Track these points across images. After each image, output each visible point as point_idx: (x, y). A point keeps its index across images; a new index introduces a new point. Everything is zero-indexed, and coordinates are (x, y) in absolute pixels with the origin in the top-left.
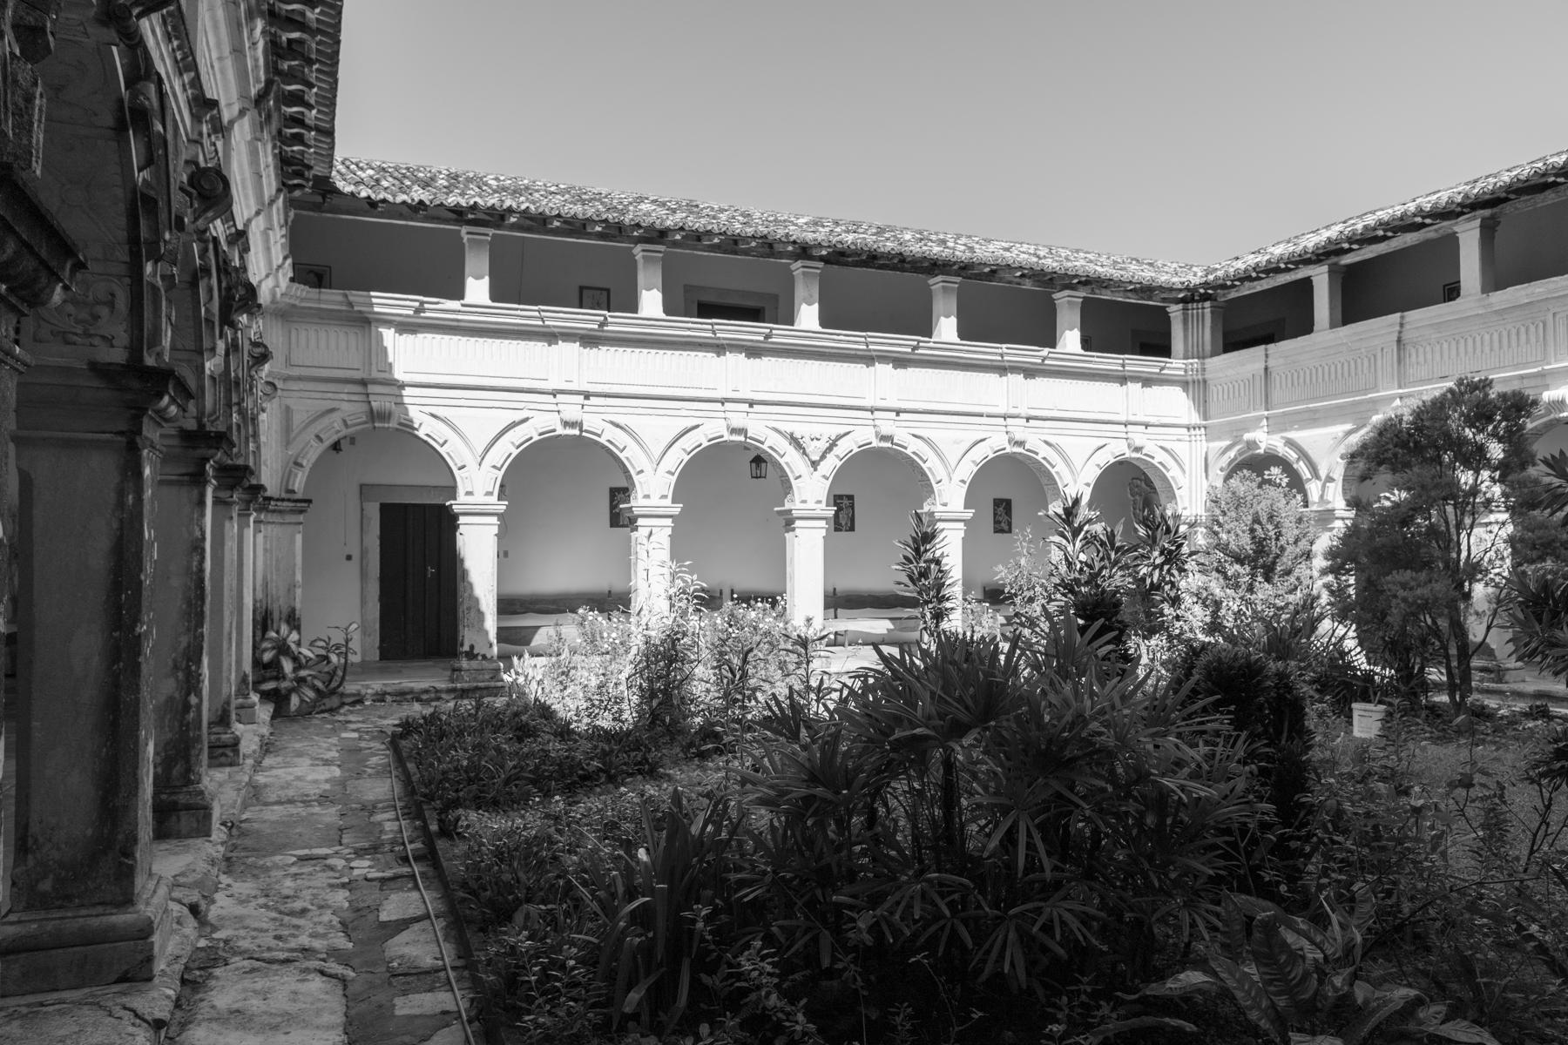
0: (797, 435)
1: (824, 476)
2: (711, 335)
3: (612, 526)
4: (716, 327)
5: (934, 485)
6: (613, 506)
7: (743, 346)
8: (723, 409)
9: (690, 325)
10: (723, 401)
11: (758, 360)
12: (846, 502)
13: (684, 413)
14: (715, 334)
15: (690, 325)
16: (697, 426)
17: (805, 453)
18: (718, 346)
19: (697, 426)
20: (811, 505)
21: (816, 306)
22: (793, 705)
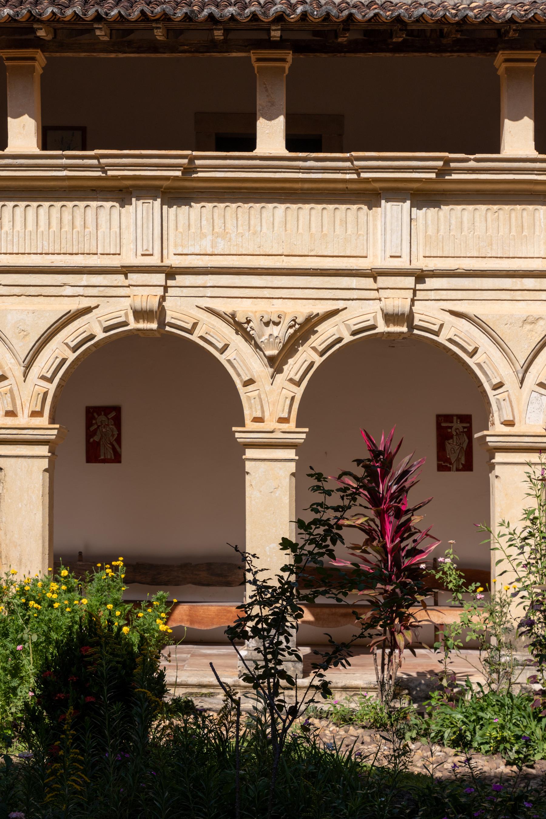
0: (241, 318)
1: (291, 380)
2: (100, 174)
3: (89, 460)
4: (103, 161)
5: (490, 393)
6: (89, 435)
7: (157, 188)
8: (127, 283)
9: (64, 161)
10: (126, 271)
11: (185, 208)
12: (457, 425)
13: (68, 291)
14: (105, 172)
15: (64, 161)
16: (88, 310)
17: (257, 346)
18: (120, 190)
19: (88, 310)
20: (270, 424)
21: (281, 119)
22: (293, 735)
